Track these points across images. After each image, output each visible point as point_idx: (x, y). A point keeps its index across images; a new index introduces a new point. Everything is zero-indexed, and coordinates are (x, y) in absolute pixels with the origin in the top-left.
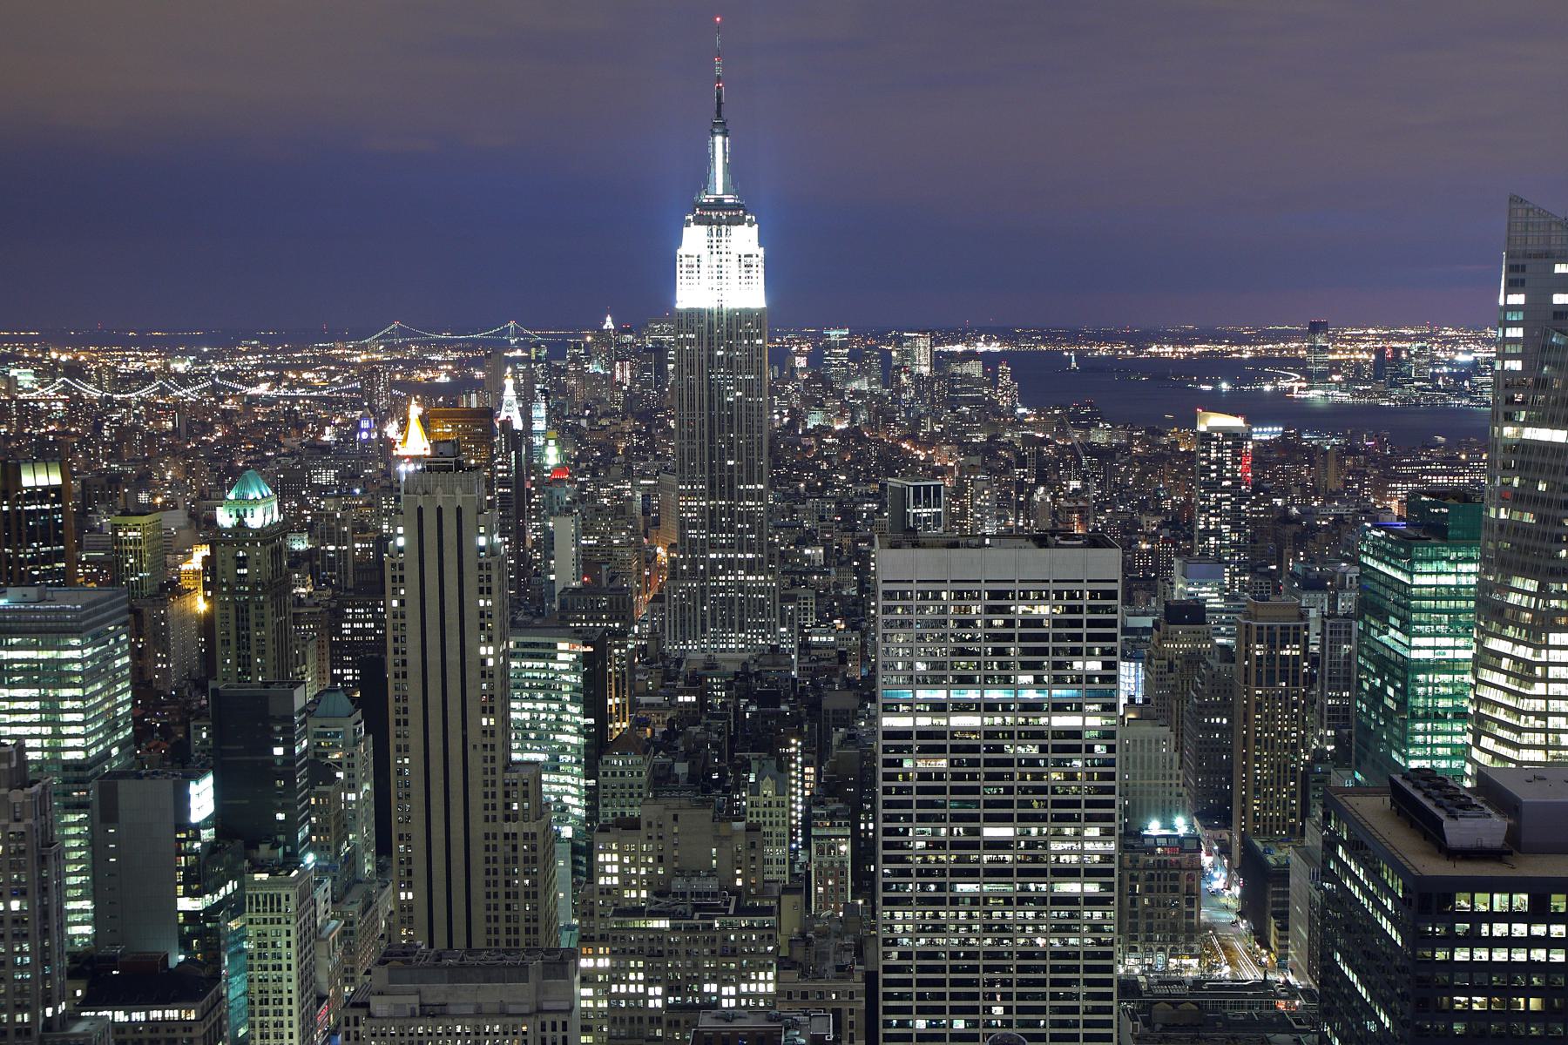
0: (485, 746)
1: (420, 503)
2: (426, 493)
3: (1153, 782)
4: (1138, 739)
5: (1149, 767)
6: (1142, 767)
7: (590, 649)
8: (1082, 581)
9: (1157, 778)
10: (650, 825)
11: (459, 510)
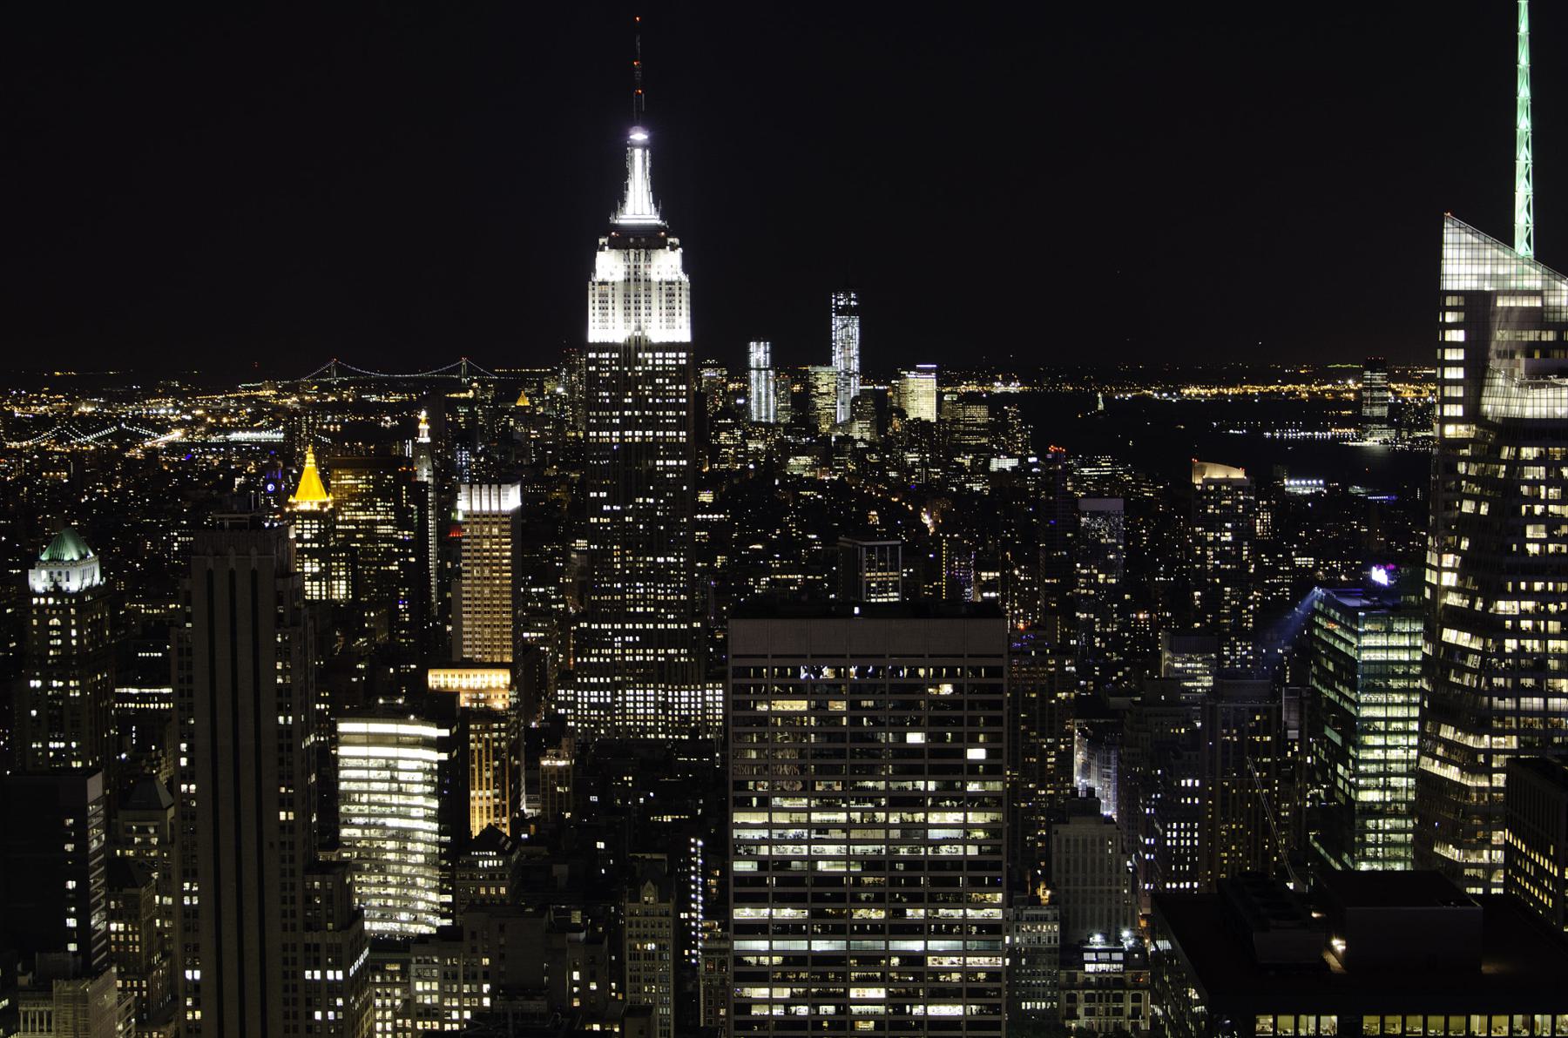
0: (283, 844)
1: (210, 564)
2: (216, 554)
3: (1097, 888)
4: (1080, 838)
5: (1093, 871)
6: (1085, 871)
7: (445, 733)
8: (962, 656)
9: (1101, 883)
10: (473, 935)
11: (254, 573)
